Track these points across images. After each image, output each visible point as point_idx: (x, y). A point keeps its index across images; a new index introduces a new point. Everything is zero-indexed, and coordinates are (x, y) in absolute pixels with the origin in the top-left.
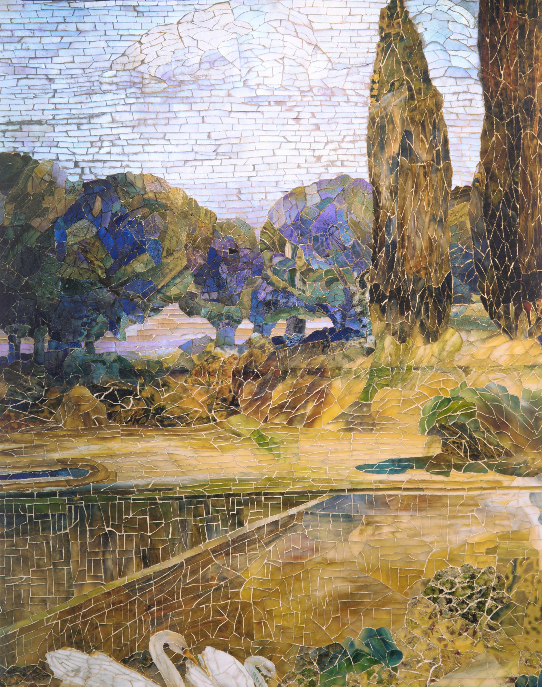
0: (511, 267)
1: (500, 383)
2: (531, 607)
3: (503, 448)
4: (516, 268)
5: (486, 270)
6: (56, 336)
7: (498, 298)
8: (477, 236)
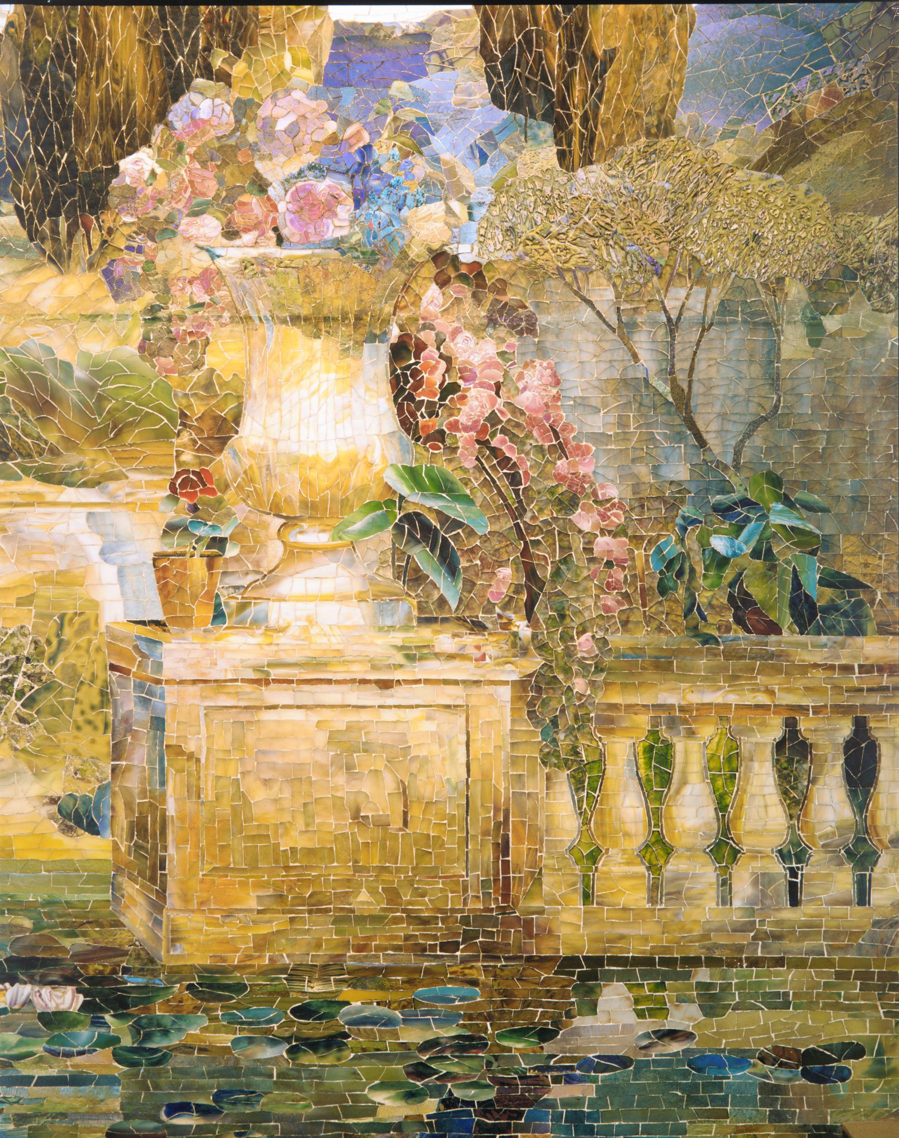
0: (63, 161)
1: (43, 342)
2: (84, 688)
3: (46, 442)
4: (71, 163)
5: (23, 164)
7: (42, 207)
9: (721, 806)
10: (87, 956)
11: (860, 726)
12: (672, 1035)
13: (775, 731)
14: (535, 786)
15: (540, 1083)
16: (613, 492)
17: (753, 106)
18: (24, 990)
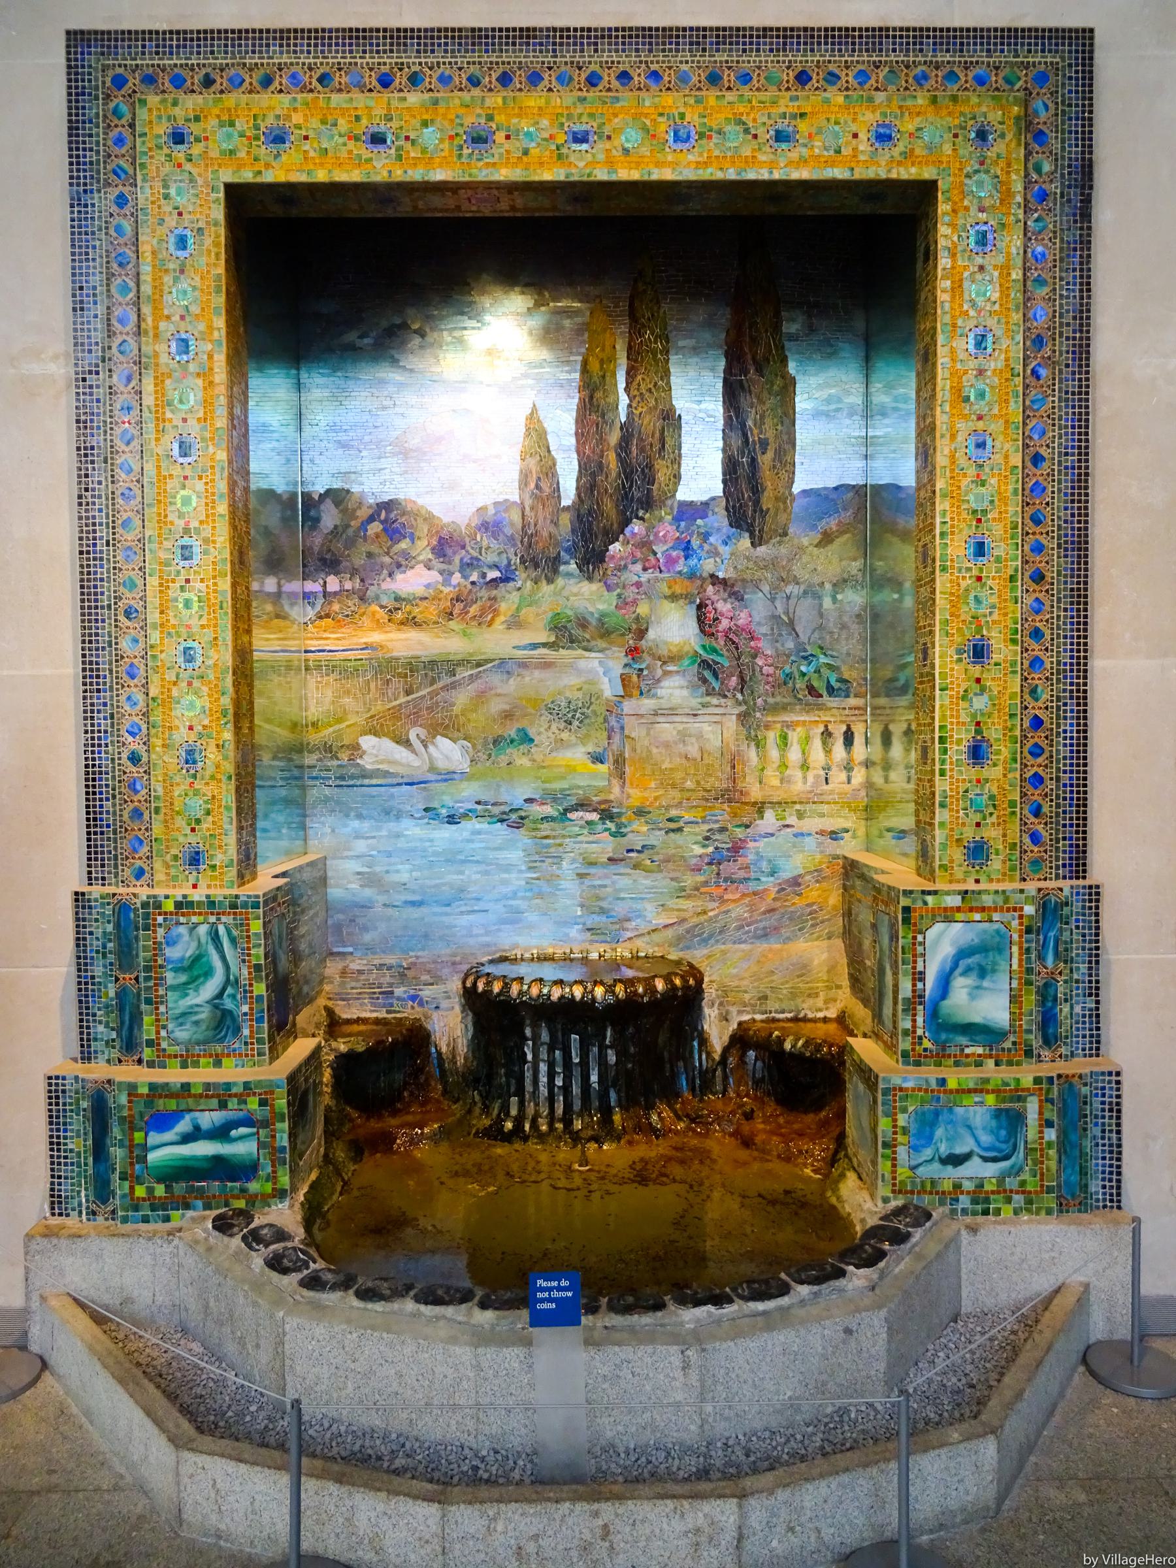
6: (362, 580)
8: (573, 531)
9: (804, 753)
10: (600, 803)
11: (849, 727)
12: (788, 826)
13: (821, 729)
14: (744, 747)
15: (744, 841)
16: (769, 652)
17: (813, 527)
18: (581, 814)
